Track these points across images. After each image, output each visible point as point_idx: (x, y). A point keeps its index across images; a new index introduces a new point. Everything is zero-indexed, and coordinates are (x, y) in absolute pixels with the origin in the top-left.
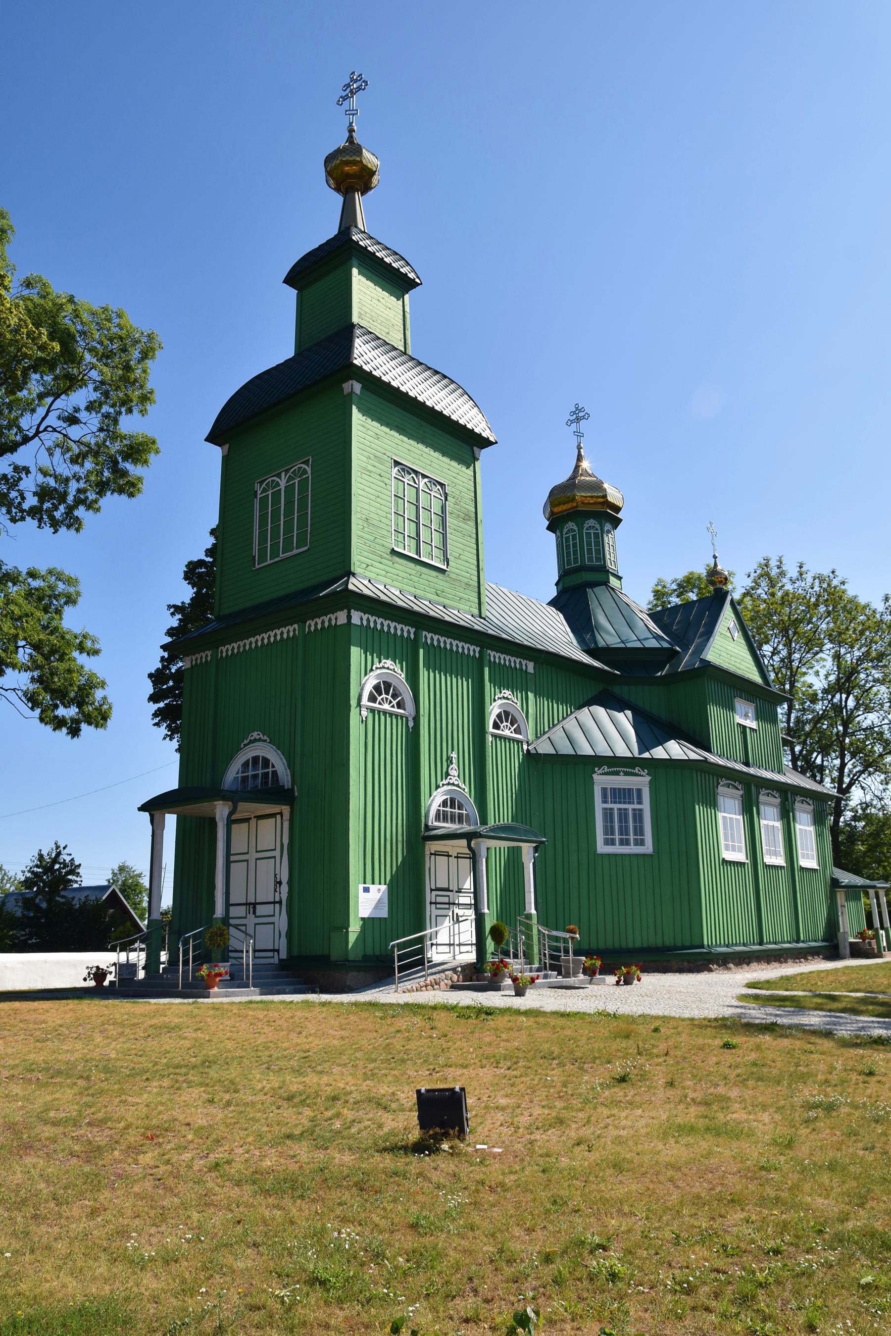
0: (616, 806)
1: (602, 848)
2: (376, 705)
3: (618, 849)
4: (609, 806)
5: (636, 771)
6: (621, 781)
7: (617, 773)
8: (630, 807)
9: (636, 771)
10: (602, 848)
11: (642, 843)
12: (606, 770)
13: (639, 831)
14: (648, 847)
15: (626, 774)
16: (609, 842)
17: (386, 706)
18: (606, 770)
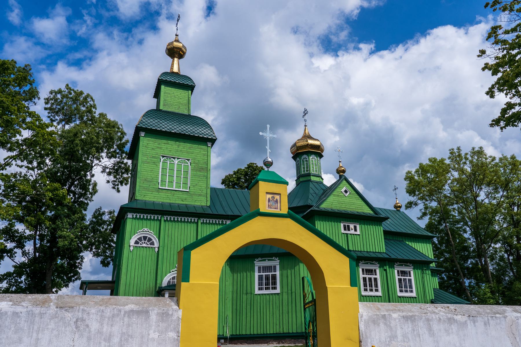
0: (264, 274)
1: (257, 291)
2: (139, 245)
3: (264, 292)
4: (262, 274)
5: (273, 258)
6: (267, 263)
7: (265, 260)
8: (270, 274)
9: (273, 258)
10: (257, 291)
11: (275, 288)
12: (260, 259)
13: (274, 283)
14: (278, 291)
15: (269, 260)
16: (259, 289)
17: (144, 245)
18: (260, 259)
